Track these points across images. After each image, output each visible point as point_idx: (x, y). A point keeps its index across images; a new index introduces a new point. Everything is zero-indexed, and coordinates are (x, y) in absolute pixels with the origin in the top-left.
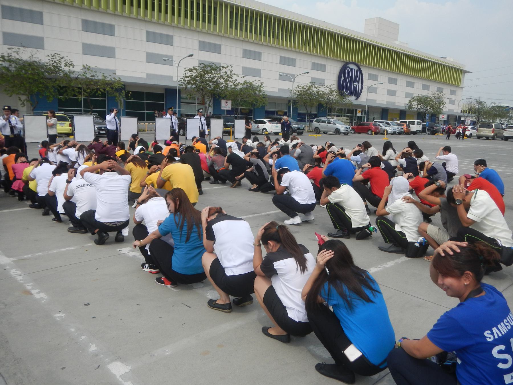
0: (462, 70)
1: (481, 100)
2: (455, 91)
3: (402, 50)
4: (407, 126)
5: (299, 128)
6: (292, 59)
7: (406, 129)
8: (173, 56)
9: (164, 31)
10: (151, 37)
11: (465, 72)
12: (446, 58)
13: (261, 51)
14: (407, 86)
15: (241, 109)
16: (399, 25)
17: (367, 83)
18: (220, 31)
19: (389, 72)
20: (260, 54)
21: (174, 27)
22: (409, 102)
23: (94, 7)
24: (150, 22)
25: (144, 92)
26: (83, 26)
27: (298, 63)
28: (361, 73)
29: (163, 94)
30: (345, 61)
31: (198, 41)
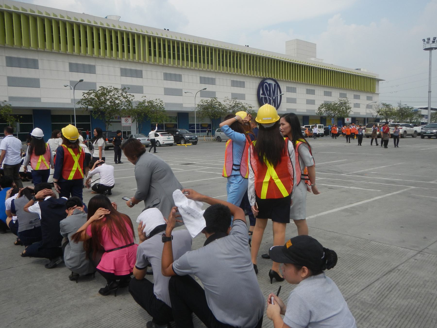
0: (375, 79)
1: (387, 104)
2: (372, 97)
3: (316, 65)
4: (308, 130)
5: (191, 139)
6: (212, 79)
7: (308, 133)
8: (96, 83)
9: (87, 62)
10: (73, 68)
11: (379, 80)
12: (360, 69)
13: (181, 74)
14: (324, 95)
15: (165, 125)
16: (316, 44)
17: (286, 95)
18: (139, 58)
19: (306, 84)
20: (180, 76)
21: (95, 58)
22: (319, 109)
23: (16, 45)
24: (72, 55)
25: (70, 115)
26: (7, 62)
27: (217, 81)
28: (278, 86)
29: (89, 115)
30: (262, 77)
31: (120, 68)
